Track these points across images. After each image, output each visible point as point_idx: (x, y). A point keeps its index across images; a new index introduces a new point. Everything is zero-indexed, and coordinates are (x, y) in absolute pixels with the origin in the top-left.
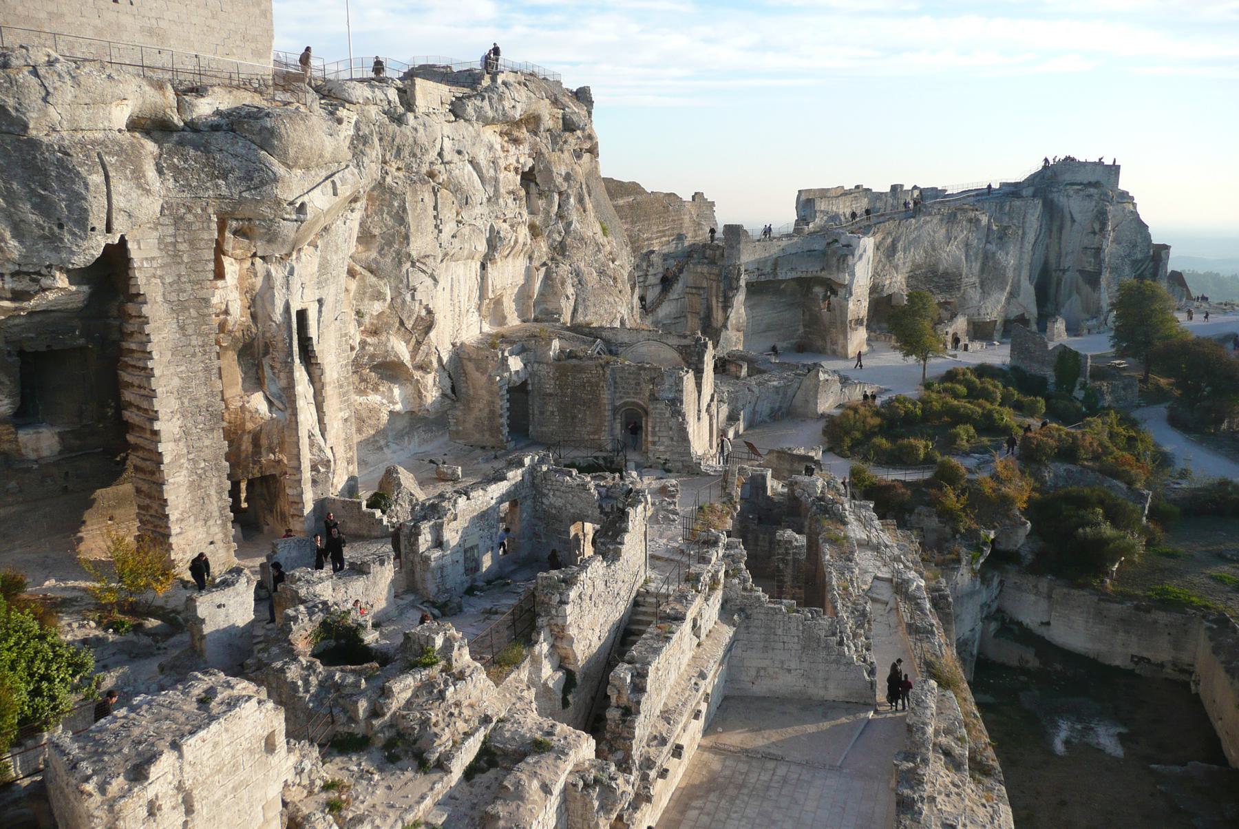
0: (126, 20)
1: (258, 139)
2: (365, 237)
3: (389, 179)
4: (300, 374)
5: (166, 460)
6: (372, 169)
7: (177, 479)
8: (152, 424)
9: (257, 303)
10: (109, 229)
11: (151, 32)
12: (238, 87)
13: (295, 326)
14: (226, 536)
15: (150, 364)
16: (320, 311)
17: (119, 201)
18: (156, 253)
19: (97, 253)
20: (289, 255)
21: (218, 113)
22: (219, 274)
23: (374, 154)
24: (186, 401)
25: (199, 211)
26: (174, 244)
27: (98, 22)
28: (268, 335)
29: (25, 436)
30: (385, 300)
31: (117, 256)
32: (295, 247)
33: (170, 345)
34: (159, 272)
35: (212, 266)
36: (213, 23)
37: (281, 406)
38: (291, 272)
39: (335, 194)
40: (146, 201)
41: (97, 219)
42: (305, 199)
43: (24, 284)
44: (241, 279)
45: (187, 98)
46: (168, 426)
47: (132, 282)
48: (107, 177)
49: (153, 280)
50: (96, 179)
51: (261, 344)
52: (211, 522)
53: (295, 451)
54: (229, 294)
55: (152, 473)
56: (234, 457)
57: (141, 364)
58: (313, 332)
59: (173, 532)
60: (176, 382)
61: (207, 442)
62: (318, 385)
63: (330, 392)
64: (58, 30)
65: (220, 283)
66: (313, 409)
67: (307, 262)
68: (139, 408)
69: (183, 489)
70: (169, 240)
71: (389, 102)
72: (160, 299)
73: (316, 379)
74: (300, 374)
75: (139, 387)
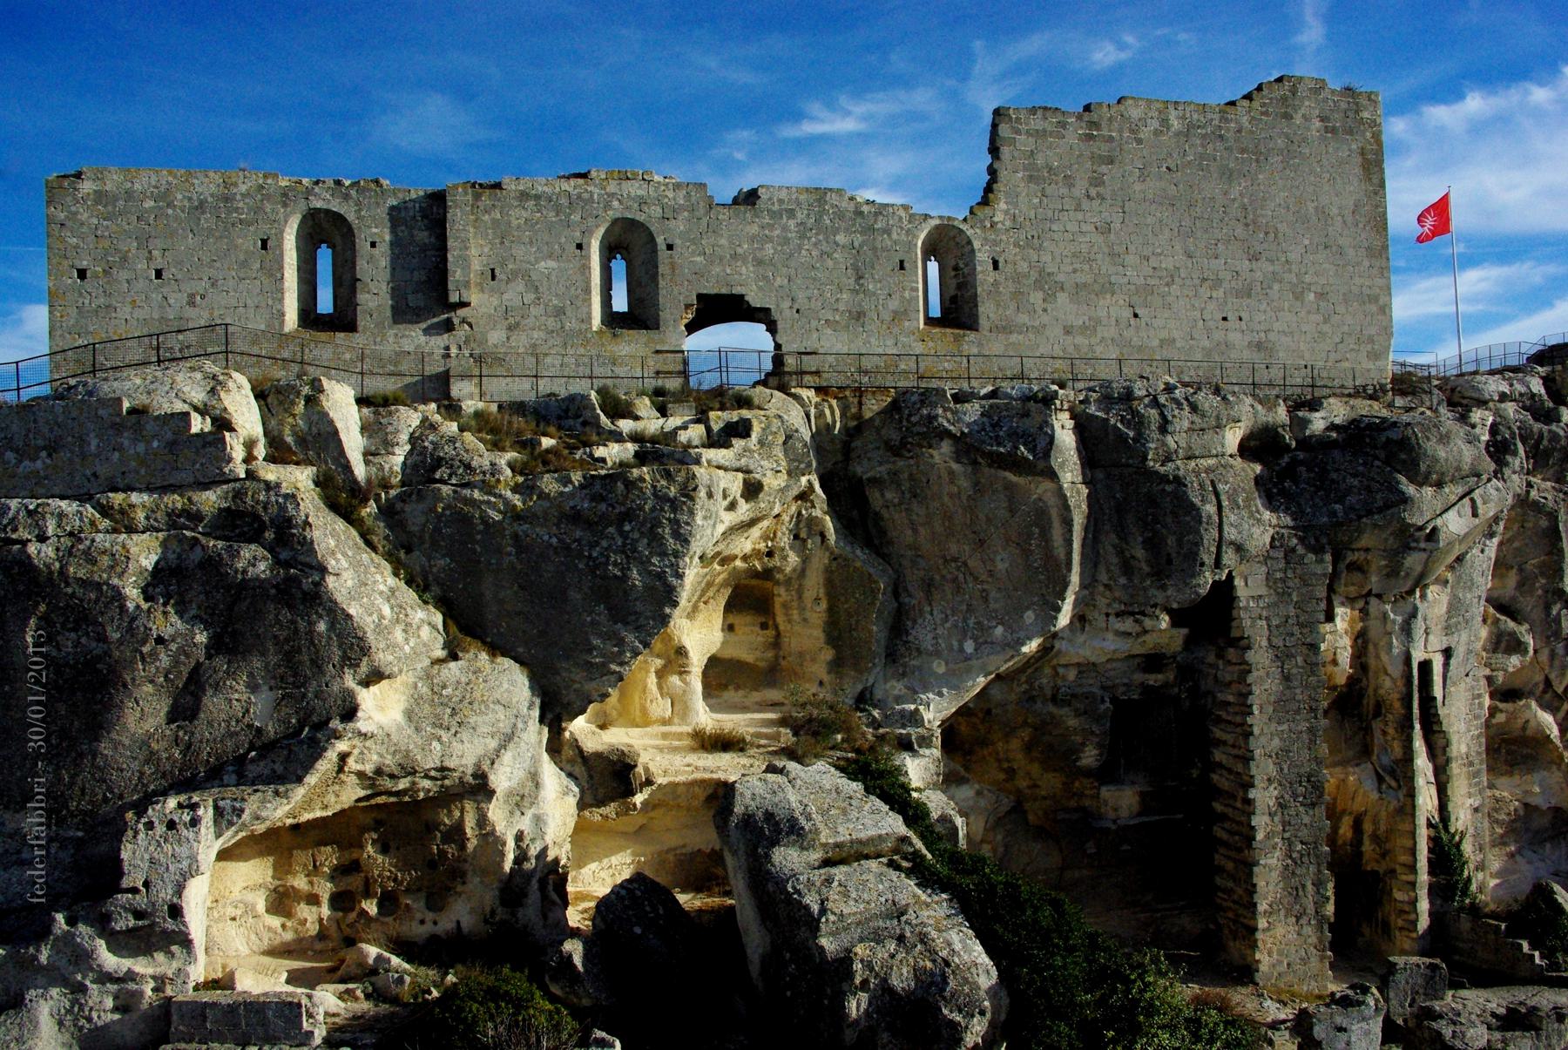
0: (1234, 337)
1: (1382, 454)
2: (1500, 566)
3: (1534, 494)
4: (1419, 744)
5: (1260, 836)
6: (1516, 482)
7: (1270, 861)
8: (1246, 792)
10: (1218, 564)
11: (1259, 346)
12: (1349, 395)
13: (1416, 682)
14: (1320, 940)
15: (1249, 720)
16: (1446, 665)
17: (1231, 533)
18: (1263, 591)
19: (1203, 591)
20: (1411, 592)
21: (1332, 427)
22: (1330, 617)
23: (1517, 462)
24: (1285, 767)
25: (1313, 542)
26: (1283, 580)
27: (1207, 343)
28: (1382, 692)
29: (1105, 792)
30: (1526, 651)
31: (1224, 591)
32: (1420, 582)
33: (1272, 699)
34: (1265, 614)
35: (1323, 605)
36: (1326, 328)
37: (1393, 784)
38: (1413, 614)
39: (1475, 514)
40: (1256, 531)
42: (1439, 522)
43: (1128, 625)
44: (1352, 622)
45: (1300, 414)
46: (1264, 796)
47: (1234, 624)
48: (1220, 507)
49: (1259, 622)
50: (1210, 508)
51: (1372, 702)
52: (1304, 921)
53: (1409, 844)
54: (1339, 634)
55: (1240, 850)
56: (1332, 840)
57: (1238, 719)
58: (1438, 691)
59: (1260, 926)
60: (1276, 742)
61: (1306, 820)
62: (1441, 760)
63: (1456, 769)
64: (1169, 357)
65: (1328, 627)
66: (1433, 790)
67: (1435, 603)
68: (1230, 771)
69: (1275, 875)
70: (1279, 575)
71: (1533, 395)
72: (1264, 643)
73: (1439, 752)
74: (1419, 744)
75: (1234, 746)
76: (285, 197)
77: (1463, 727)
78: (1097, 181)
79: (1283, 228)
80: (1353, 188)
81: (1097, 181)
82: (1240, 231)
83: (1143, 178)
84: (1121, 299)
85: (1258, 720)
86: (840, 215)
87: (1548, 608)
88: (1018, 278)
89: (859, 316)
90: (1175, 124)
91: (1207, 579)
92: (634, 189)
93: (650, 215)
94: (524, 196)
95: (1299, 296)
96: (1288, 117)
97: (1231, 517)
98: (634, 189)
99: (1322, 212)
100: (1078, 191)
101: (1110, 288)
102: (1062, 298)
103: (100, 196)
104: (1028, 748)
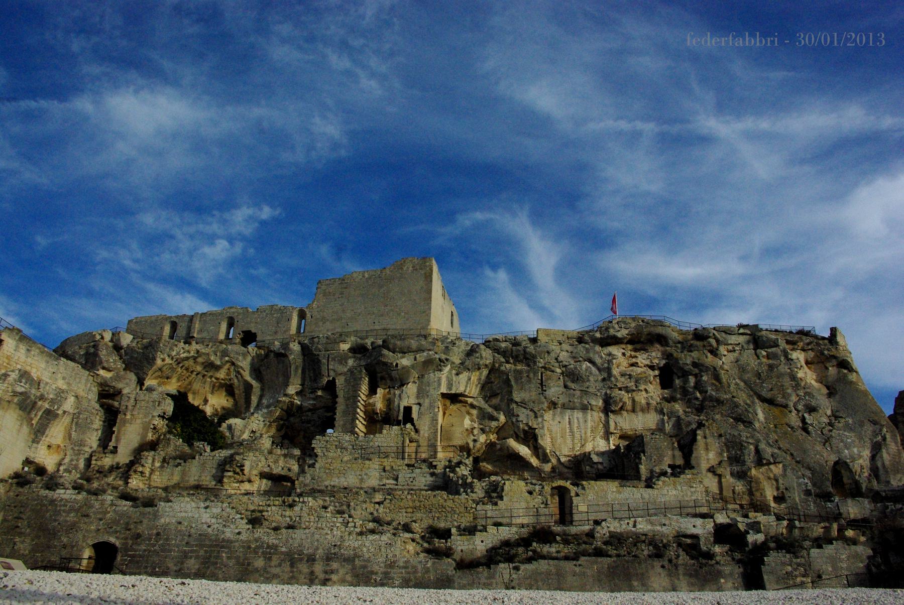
9: (389, 402)
17: (331, 367)
19: (325, 382)
31: (331, 385)
41: (324, 371)
43: (312, 396)
44: (384, 396)
50: (324, 361)
58: (415, 415)
77: (426, 428)
78: (342, 293)
80: (422, 283)
81: (342, 293)
85: (338, 416)
87: (508, 405)
89: (276, 333)
92: (233, 310)
93: (234, 316)
95: (399, 314)
98: (233, 310)
100: (337, 295)
102: (328, 323)
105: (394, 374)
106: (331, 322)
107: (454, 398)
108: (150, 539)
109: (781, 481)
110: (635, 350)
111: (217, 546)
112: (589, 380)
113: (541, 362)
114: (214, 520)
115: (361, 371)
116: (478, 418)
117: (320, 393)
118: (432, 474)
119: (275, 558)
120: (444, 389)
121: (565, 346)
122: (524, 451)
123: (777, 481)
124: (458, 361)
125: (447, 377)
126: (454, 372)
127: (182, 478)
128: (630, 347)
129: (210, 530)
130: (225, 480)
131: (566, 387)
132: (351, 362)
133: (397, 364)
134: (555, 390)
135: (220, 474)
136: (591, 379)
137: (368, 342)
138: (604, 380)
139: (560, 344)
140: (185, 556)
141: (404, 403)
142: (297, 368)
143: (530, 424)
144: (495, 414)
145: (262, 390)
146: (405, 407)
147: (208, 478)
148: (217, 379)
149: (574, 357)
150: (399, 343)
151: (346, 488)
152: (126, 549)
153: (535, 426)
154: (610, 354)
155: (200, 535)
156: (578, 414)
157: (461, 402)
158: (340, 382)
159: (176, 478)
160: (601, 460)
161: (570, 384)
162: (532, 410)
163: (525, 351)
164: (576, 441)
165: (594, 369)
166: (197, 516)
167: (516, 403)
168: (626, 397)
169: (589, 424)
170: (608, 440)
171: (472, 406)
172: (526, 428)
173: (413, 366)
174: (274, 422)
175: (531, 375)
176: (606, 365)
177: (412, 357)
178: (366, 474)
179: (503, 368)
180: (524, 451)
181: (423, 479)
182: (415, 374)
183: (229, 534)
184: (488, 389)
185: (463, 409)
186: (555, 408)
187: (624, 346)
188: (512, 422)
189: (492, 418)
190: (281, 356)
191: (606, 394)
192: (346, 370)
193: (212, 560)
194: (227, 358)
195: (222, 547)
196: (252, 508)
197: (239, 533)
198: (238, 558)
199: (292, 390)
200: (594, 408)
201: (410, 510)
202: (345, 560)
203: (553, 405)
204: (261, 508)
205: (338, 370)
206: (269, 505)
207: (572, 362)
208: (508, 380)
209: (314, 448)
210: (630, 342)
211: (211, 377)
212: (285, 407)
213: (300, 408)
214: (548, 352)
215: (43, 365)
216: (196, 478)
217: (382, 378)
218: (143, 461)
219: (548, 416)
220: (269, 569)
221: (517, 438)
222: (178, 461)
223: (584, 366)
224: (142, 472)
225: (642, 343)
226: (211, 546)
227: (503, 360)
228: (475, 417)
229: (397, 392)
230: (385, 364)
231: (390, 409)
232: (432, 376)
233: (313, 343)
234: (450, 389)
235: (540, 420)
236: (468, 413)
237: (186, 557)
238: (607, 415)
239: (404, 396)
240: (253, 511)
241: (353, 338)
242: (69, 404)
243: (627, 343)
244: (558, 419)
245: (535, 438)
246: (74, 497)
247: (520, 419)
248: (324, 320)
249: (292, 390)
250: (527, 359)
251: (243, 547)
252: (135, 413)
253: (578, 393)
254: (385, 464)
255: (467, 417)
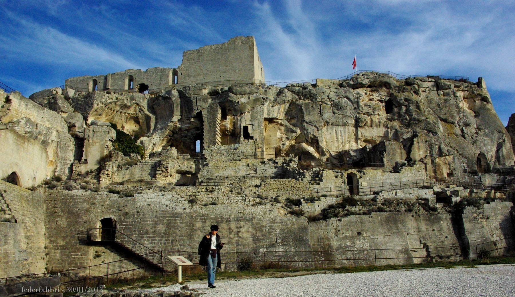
9: (234, 124)
17: (198, 104)
41: (195, 107)
43: (188, 122)
44: (231, 120)
50: (194, 101)
58: (250, 131)
76: (90, 78)
78: (199, 59)
79: (233, 61)
80: (247, 52)
81: (199, 59)
82: (224, 62)
83: (207, 57)
84: (202, 76)
85: (205, 133)
86: (159, 70)
87: (302, 124)
88: (185, 75)
89: (160, 84)
90: (213, 48)
91: (195, 112)
92: (131, 71)
93: (133, 75)
94: (117, 74)
95: (235, 71)
96: (235, 43)
97: (198, 102)
98: (131, 71)
99: (241, 57)
101: (200, 75)
102: (192, 78)
103: (70, 81)
104: (184, 146)
105: (237, 107)
106: (194, 76)
107: (271, 120)
108: (134, 215)
109: (451, 165)
110: (372, 91)
111: (173, 216)
112: (347, 109)
113: (319, 99)
114: (169, 202)
115: (217, 107)
116: (284, 131)
117: (192, 120)
118: (276, 167)
119: (207, 221)
120: (266, 116)
121: (333, 89)
122: (311, 150)
123: (449, 165)
124: (273, 99)
125: (267, 108)
126: (271, 105)
127: (131, 176)
128: (369, 89)
129: (167, 208)
130: (157, 176)
131: (334, 113)
132: (210, 101)
133: (238, 102)
134: (328, 115)
135: (153, 173)
136: (348, 108)
137: (219, 88)
138: (355, 108)
139: (330, 87)
140: (156, 223)
141: (243, 124)
142: (177, 106)
143: (315, 134)
144: (294, 129)
145: (156, 119)
146: (244, 127)
147: (147, 175)
148: (129, 114)
149: (338, 96)
150: (239, 89)
151: (227, 177)
152: (121, 222)
153: (317, 136)
154: (358, 94)
155: (162, 211)
156: (340, 128)
157: (275, 122)
158: (204, 113)
159: (127, 177)
160: (355, 154)
161: (336, 111)
162: (315, 126)
163: (310, 92)
164: (340, 144)
165: (349, 102)
166: (158, 200)
167: (307, 122)
168: (368, 119)
169: (347, 134)
170: (357, 142)
171: (281, 125)
172: (312, 137)
173: (248, 103)
174: (165, 137)
175: (314, 106)
176: (356, 100)
177: (247, 97)
178: (238, 169)
179: (298, 102)
180: (311, 150)
181: (271, 170)
182: (249, 107)
183: (179, 209)
184: (289, 115)
185: (276, 127)
186: (328, 125)
187: (365, 89)
188: (304, 134)
189: (293, 131)
190: (167, 98)
191: (356, 117)
192: (207, 106)
193: (172, 224)
194: (134, 101)
195: (177, 217)
196: (189, 194)
197: (185, 209)
198: (187, 223)
199: (176, 118)
200: (350, 125)
201: (275, 190)
202: (247, 220)
203: (327, 123)
204: (194, 194)
205: (204, 105)
206: (199, 192)
207: (337, 98)
208: (301, 109)
209: (204, 155)
210: (369, 86)
211: (125, 113)
212: (172, 129)
213: (180, 129)
214: (323, 93)
215: (36, 114)
216: (139, 176)
217: (229, 110)
218: (107, 168)
219: (324, 129)
220: (205, 228)
221: (307, 142)
222: (127, 166)
223: (344, 101)
224: (107, 174)
225: (376, 87)
226: (170, 217)
227: (297, 97)
228: (283, 131)
229: (239, 118)
230: (231, 102)
231: (235, 128)
232: (259, 108)
233: (186, 90)
234: (269, 115)
235: (320, 132)
236: (279, 129)
237: (157, 224)
238: (357, 129)
239: (243, 120)
240: (190, 196)
241: (210, 87)
242: (54, 136)
243: (367, 87)
244: (330, 131)
245: (318, 142)
246: (84, 193)
247: (309, 131)
248: (189, 76)
249: (176, 118)
250: (311, 96)
251: (189, 216)
252: (95, 139)
253: (341, 116)
254: (248, 162)
255: (279, 131)
